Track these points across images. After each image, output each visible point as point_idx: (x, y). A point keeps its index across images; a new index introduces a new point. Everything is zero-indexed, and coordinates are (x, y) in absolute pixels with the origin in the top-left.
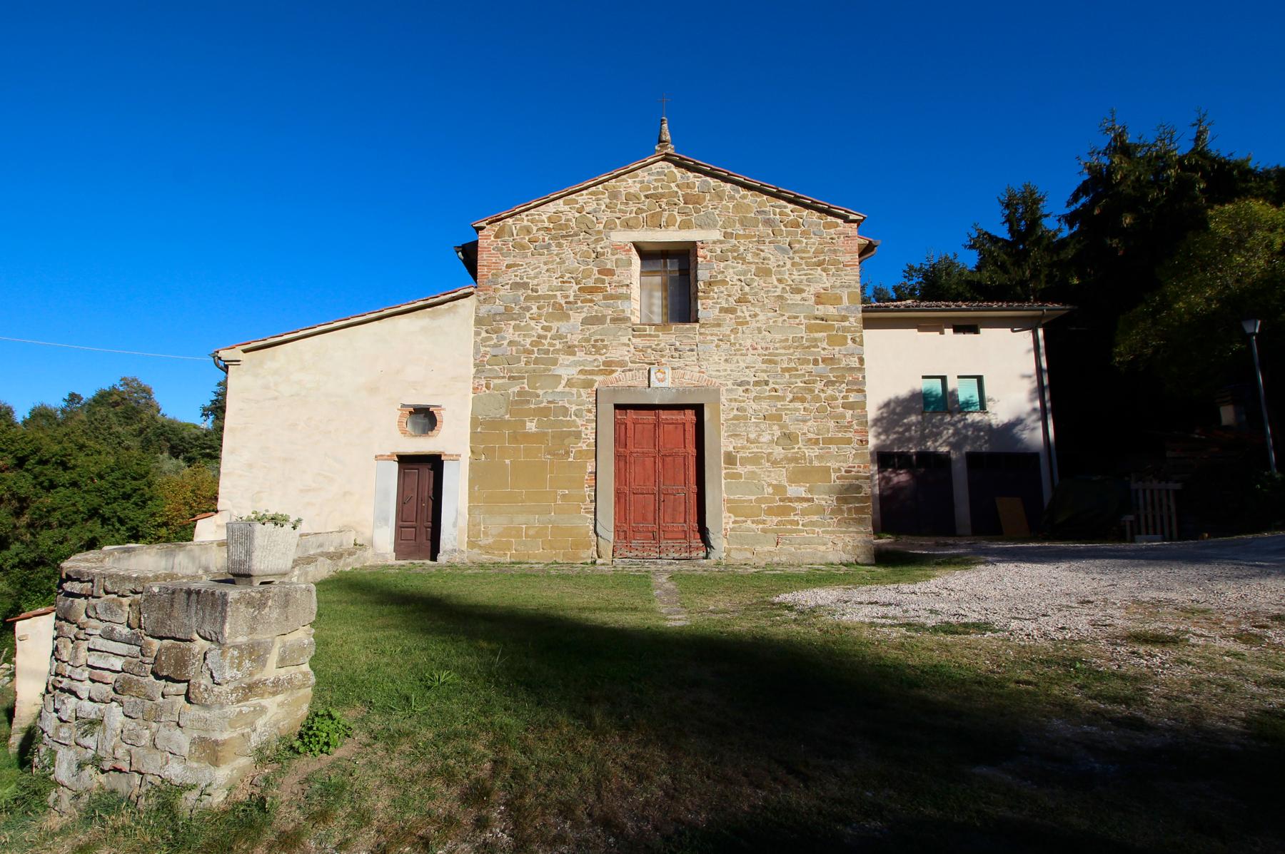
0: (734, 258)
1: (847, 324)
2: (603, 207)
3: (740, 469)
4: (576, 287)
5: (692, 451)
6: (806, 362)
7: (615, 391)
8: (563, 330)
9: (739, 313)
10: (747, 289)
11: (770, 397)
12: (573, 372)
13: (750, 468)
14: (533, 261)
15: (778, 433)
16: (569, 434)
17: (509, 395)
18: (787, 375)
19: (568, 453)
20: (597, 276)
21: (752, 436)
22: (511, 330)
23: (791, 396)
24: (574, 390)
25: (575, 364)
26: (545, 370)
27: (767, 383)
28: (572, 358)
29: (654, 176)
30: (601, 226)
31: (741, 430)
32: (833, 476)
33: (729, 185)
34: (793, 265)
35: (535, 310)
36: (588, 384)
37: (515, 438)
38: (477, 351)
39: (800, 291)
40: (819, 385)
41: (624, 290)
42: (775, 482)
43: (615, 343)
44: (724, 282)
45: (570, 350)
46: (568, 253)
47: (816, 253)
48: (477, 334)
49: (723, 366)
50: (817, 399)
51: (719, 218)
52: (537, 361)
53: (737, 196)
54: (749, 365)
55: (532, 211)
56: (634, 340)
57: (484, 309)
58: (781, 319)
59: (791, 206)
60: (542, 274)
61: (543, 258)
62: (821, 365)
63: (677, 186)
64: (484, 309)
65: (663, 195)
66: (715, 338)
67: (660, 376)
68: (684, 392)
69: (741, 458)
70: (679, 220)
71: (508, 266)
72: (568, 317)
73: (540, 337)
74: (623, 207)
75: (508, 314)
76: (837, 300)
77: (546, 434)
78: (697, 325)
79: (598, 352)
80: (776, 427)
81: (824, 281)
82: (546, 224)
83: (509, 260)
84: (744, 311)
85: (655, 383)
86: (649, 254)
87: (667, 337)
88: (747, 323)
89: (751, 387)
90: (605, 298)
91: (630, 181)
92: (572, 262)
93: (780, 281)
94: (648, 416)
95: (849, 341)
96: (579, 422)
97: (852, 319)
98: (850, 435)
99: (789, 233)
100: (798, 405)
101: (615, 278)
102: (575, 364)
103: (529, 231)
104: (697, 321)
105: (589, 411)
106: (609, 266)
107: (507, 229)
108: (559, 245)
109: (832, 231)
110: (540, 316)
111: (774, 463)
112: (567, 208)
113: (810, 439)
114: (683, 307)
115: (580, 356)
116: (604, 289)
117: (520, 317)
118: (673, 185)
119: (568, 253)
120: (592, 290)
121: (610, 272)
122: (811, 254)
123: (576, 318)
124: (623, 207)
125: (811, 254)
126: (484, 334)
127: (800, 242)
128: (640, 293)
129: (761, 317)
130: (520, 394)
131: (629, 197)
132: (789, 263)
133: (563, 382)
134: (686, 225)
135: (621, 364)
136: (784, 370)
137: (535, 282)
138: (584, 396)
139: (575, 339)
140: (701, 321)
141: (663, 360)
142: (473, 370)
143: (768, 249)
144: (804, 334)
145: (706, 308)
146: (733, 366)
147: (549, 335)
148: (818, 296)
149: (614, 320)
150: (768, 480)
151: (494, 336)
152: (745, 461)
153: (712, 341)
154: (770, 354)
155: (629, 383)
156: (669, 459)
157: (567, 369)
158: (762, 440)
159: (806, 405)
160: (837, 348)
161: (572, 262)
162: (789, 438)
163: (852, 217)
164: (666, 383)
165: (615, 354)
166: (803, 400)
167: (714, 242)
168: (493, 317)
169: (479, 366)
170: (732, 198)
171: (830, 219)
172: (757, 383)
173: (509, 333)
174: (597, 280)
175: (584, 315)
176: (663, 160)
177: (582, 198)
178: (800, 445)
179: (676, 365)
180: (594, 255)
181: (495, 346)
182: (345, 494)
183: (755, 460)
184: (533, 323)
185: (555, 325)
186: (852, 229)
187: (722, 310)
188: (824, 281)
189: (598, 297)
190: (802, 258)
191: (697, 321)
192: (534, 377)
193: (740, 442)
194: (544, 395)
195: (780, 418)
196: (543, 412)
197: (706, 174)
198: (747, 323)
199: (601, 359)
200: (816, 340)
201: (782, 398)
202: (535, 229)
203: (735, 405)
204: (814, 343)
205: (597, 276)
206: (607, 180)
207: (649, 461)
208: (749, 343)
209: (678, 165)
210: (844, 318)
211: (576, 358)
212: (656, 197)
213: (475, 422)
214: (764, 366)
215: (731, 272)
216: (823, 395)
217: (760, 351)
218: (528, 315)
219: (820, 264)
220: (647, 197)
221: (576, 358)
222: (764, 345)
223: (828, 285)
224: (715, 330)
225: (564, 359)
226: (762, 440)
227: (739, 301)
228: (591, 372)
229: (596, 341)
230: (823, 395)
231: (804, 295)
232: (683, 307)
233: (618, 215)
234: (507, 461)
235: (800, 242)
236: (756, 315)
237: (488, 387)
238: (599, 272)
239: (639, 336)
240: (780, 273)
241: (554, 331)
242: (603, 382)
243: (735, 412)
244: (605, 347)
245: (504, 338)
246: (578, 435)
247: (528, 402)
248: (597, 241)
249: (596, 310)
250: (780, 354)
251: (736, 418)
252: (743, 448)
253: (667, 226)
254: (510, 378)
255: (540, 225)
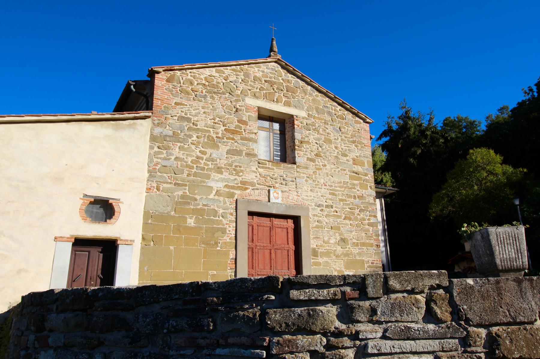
0: (314, 130)
1: (367, 178)
2: (240, 81)
3: (320, 260)
4: (223, 128)
5: (292, 247)
6: (350, 197)
7: (249, 202)
8: (214, 155)
9: (317, 163)
10: (320, 149)
11: (334, 216)
12: (221, 185)
13: (325, 259)
14: (195, 104)
15: (338, 238)
16: (218, 229)
17: (174, 197)
18: (341, 203)
19: (216, 244)
20: (237, 123)
21: (326, 239)
22: (177, 149)
23: (344, 216)
24: (221, 199)
25: (223, 180)
26: (201, 182)
27: (332, 207)
28: (220, 176)
29: (267, 69)
30: (239, 92)
31: (320, 235)
32: (366, 266)
33: (309, 87)
34: (342, 140)
35: (195, 138)
36: (231, 195)
37: (178, 229)
38: (150, 161)
39: (346, 156)
40: (357, 211)
41: (253, 136)
42: (338, 269)
43: (248, 170)
44: (308, 143)
45: (219, 170)
46: (218, 105)
47: (353, 136)
48: (151, 148)
49: (310, 193)
50: (356, 219)
51: (305, 105)
52: (195, 174)
53: (314, 94)
54: (321, 195)
55: (194, 71)
56: (259, 170)
57: (158, 131)
58: (337, 170)
59: (339, 107)
60: (201, 114)
61: (201, 104)
62: (357, 200)
63: (283, 79)
64: (158, 131)
65: (275, 83)
66: (305, 176)
67: (275, 194)
68: (289, 207)
69: (321, 252)
70: (284, 100)
71: (176, 103)
72: (218, 147)
73: (198, 157)
74: (252, 84)
75: (175, 136)
76: (362, 164)
77: (201, 228)
78: (295, 166)
79: (237, 174)
80: (337, 234)
81: (355, 153)
82: (204, 82)
83: (178, 100)
84: (319, 162)
85: (273, 200)
86: (265, 116)
87: (279, 171)
88: (321, 169)
89: (324, 208)
90: (242, 139)
91: (256, 69)
92: (220, 111)
93: (336, 148)
94: (265, 221)
95: (369, 188)
96: (225, 222)
97: (369, 176)
98: (372, 242)
99: (339, 122)
100: (347, 222)
101: (248, 127)
102: (223, 180)
103: (191, 83)
104: (295, 163)
105: (231, 214)
106: (244, 119)
107: (176, 78)
108: (212, 98)
109: (358, 125)
110: (199, 143)
111: (337, 256)
112: (217, 75)
113: (354, 243)
114: (286, 153)
115: (226, 175)
116: (240, 133)
117: (184, 141)
118: (280, 78)
119: (218, 105)
120: (234, 132)
121: (245, 123)
122: (349, 136)
123: (223, 149)
124: (252, 84)
125: (349, 136)
126: (156, 149)
127: (344, 128)
128: (264, 141)
129: (328, 167)
130: (183, 197)
131: (255, 79)
132: (340, 138)
133: (214, 192)
134: (288, 104)
135: (252, 184)
136: (341, 200)
137: (196, 119)
138: (228, 203)
139: (222, 163)
140: (298, 164)
141: (277, 185)
142: (147, 175)
143: (330, 129)
144: (348, 180)
145: (301, 157)
146: (315, 194)
147: (205, 157)
148: (354, 160)
149: (248, 155)
150: (334, 267)
151: (165, 152)
152: (323, 254)
153: (303, 177)
154: (333, 190)
155: (257, 198)
156: (279, 252)
157: (217, 183)
158: (331, 241)
159: (351, 222)
160: (364, 191)
161: (220, 111)
162: (343, 240)
163: (368, 120)
164: (279, 201)
165: (250, 177)
166: (350, 219)
167: (303, 118)
168: (165, 138)
169: (152, 173)
170: (311, 95)
171: (357, 119)
172: (327, 206)
173: (176, 152)
174: (237, 126)
175: (228, 148)
176: (275, 62)
177: (227, 71)
178: (349, 246)
179: (284, 189)
180: (234, 110)
181: (165, 159)
182: (19, 271)
183: (327, 254)
184: (193, 147)
185: (209, 151)
186: (367, 127)
187: (308, 159)
188: (355, 153)
189: (237, 137)
190: (346, 137)
191: (295, 163)
192: (193, 186)
193: (320, 242)
194: (201, 199)
195: (338, 228)
196: (198, 212)
197: (298, 77)
198: (321, 169)
199: (239, 179)
200: (354, 185)
201: (339, 217)
202: (196, 83)
203: (316, 218)
204: (353, 186)
205: (237, 123)
206: (243, 64)
207: (267, 252)
208: (322, 181)
209: (283, 67)
210: (366, 175)
211: (223, 176)
212: (272, 84)
213: (147, 215)
214: (330, 196)
215: (312, 137)
216: (359, 217)
217: (328, 187)
218: (190, 141)
219: (354, 142)
220: (266, 81)
221: (223, 176)
222: (330, 184)
223: (358, 155)
224: (305, 171)
225: (215, 175)
226: (331, 241)
227: (317, 155)
228: (233, 187)
229: (236, 166)
230: (359, 217)
231: (348, 158)
232: (286, 153)
233: (250, 88)
234: (172, 248)
235: (344, 128)
236: (325, 166)
237: (158, 189)
238: (238, 121)
239: (263, 168)
240: (336, 143)
241: (208, 155)
242: (241, 195)
243: (317, 223)
244: (242, 171)
245: (171, 154)
246: (224, 231)
247: (189, 203)
248: (237, 101)
249: (236, 146)
250: (338, 191)
251: (317, 227)
252: (321, 246)
253: (277, 102)
254: (175, 184)
255: (199, 81)
